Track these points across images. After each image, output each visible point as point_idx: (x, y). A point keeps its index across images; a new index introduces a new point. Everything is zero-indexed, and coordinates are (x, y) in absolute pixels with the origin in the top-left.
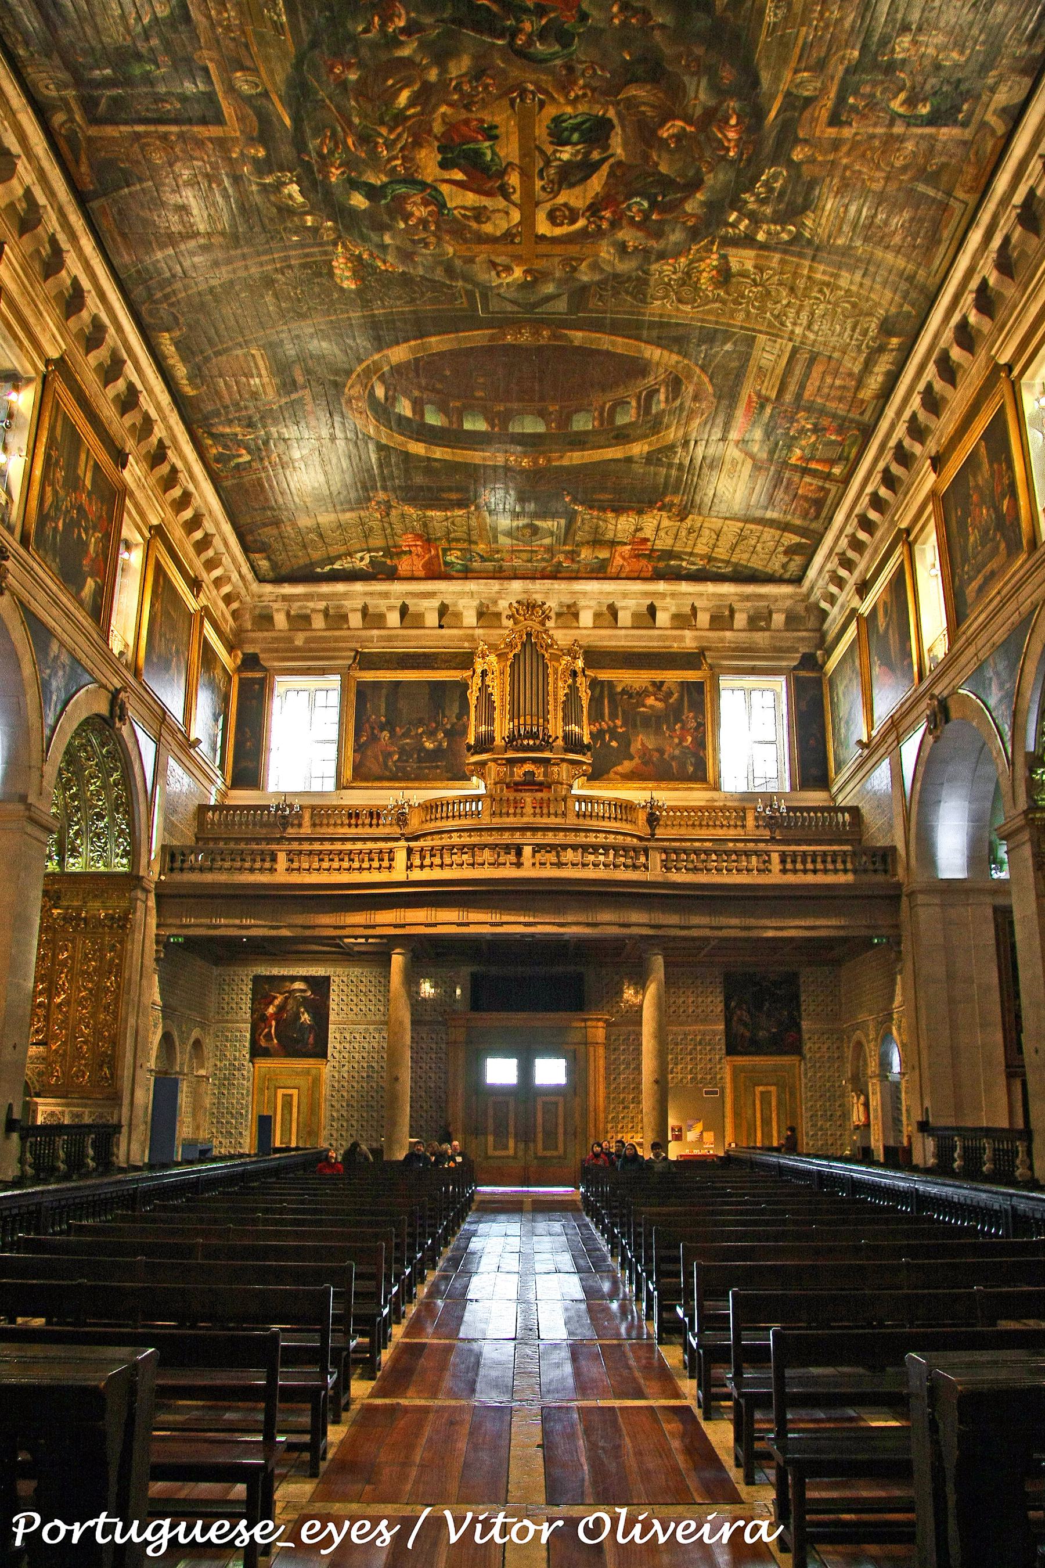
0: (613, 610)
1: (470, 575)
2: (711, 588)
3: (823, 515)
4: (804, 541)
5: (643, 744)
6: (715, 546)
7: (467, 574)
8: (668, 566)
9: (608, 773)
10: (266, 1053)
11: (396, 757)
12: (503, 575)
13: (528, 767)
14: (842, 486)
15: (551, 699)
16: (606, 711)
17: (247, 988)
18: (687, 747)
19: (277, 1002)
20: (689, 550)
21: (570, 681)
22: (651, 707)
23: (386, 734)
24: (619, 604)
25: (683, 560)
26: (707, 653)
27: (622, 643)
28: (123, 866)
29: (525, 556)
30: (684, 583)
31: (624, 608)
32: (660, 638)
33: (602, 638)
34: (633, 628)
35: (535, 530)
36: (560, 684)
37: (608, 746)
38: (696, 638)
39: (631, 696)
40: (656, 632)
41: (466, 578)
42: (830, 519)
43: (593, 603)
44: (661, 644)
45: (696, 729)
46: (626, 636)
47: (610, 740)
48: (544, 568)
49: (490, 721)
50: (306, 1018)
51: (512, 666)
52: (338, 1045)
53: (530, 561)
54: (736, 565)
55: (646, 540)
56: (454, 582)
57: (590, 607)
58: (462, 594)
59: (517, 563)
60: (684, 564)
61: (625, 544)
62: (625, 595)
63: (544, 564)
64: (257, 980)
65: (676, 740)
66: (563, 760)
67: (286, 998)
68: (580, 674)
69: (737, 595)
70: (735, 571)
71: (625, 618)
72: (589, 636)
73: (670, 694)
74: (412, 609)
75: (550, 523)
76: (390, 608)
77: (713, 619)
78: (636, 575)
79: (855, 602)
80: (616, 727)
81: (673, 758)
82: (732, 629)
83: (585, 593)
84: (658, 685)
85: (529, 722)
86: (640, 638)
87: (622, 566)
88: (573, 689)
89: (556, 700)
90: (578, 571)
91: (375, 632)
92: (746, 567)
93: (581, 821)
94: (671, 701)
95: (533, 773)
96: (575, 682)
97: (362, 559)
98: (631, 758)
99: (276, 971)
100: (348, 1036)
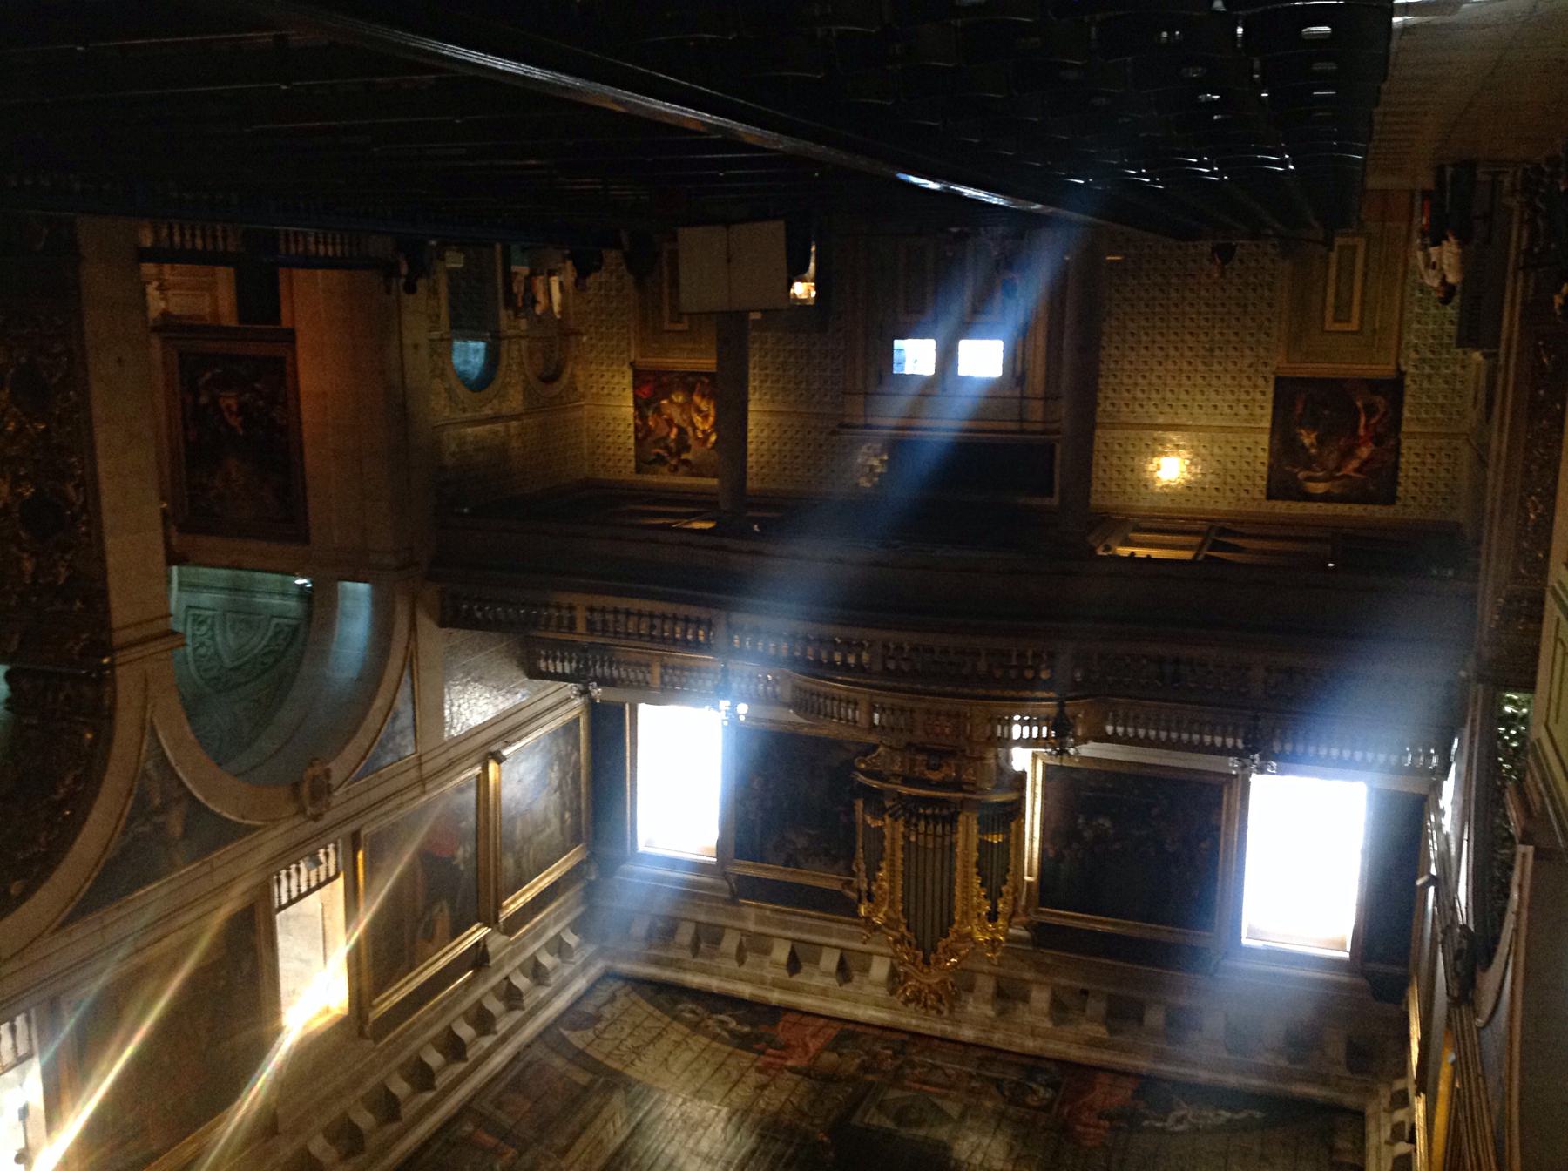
0: (844, 971)
2: (714, 984)
3: (520, 1065)
4: (566, 1033)
6: (678, 1044)
7: (1033, 1064)
8: (752, 1025)
10: (1374, 385)
11: (1155, 811)
12: (980, 1053)
13: (935, 776)
14: (475, 1105)
15: (899, 867)
17: (1405, 487)
19: (1355, 464)
20: (715, 1045)
21: (874, 888)
24: (832, 982)
25: (731, 1032)
26: (727, 896)
28: (1512, 702)
29: (937, 1077)
30: (747, 997)
31: (826, 974)
34: (821, 945)
35: (900, 1117)
38: (743, 918)
40: (790, 934)
42: (516, 1058)
43: (868, 989)
46: (830, 935)
48: (921, 1052)
49: (984, 846)
50: (1308, 439)
51: (951, 922)
52: (1259, 396)
53: (936, 1067)
54: (665, 1012)
55: (760, 1070)
56: (1056, 1055)
59: (952, 1068)
60: (733, 1024)
61: (792, 1070)
62: (824, 992)
63: (917, 1059)
64: (1391, 499)
67: (1338, 469)
68: (864, 895)
69: (685, 970)
70: (676, 1002)
71: (830, 961)
75: (875, 1122)
77: (716, 941)
78: (806, 1020)
79: (497, 942)
82: (698, 923)
83: (877, 1005)
84: (790, 861)
85: (930, 838)
87: (814, 1036)
88: (872, 878)
89: (892, 864)
90: (877, 1039)
92: (658, 1007)
93: (853, 695)
95: (929, 768)
96: (869, 885)
97: (1180, 1120)
99: (1357, 510)
100: (1243, 411)
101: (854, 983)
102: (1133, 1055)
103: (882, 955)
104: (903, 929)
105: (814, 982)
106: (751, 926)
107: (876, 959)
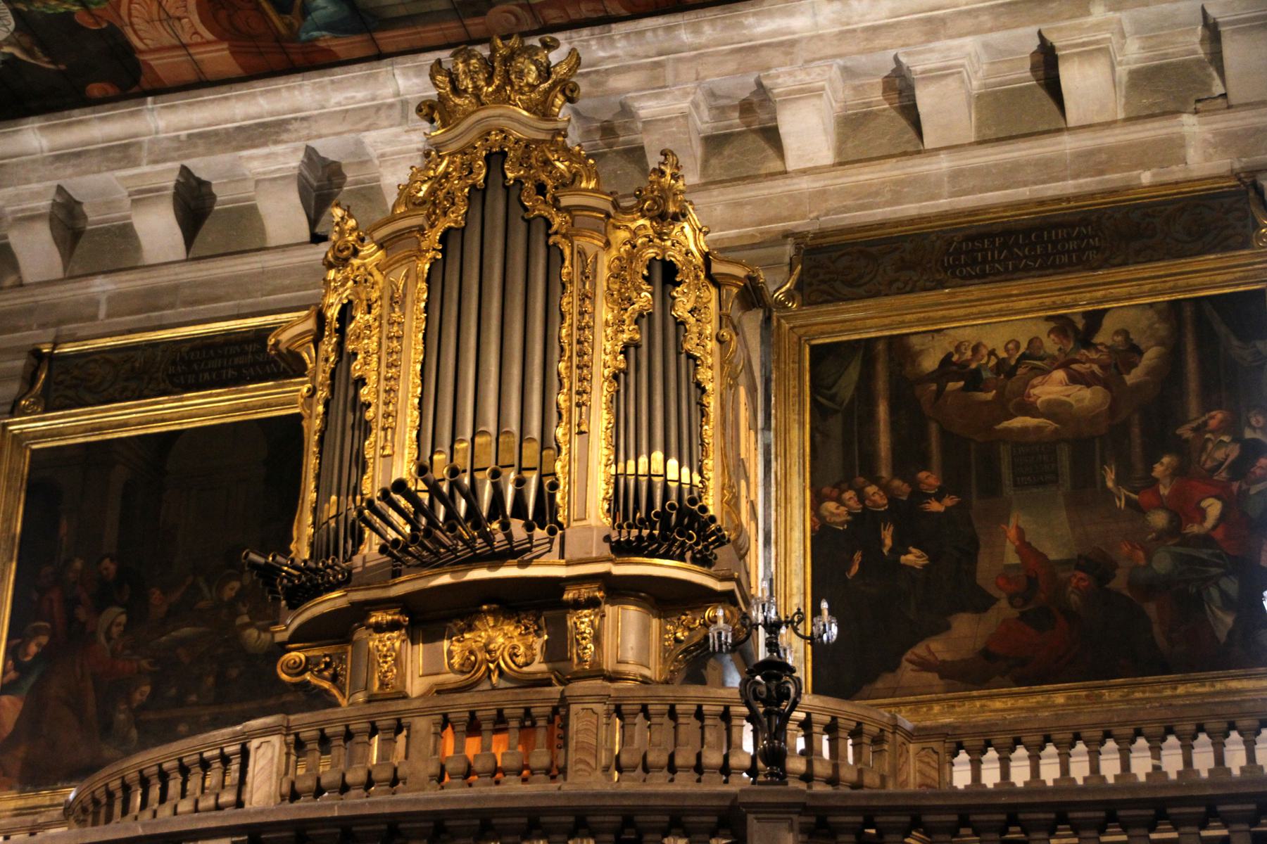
1: (387, 38)
5: (1025, 548)
9: (894, 667)
16: (884, 442)
18: (1206, 540)
21: (644, 298)
22: (1055, 410)
23: (116, 616)
24: (918, 64)
27: (944, 203)
32: (1090, 162)
33: (868, 195)
34: (981, 142)
36: (605, 312)
37: (893, 566)
38: (1227, 141)
39: (974, 380)
40: (1067, 144)
41: (379, 56)
43: (819, 75)
44: (1087, 183)
45: (1240, 468)
46: (956, 175)
47: (901, 546)
56: (340, 75)
57: (815, 92)
58: (370, 115)
65: (1159, 519)
66: (619, 590)
72: (822, 194)
73: (1133, 351)
74: (224, 195)
76: (142, 197)
80: (919, 495)
81: (1149, 588)
83: (788, 46)
86: (1009, 175)
91: (102, 286)
94: (1131, 378)
96: (667, 302)
98: (980, 602)
101: (879, 80)
102: (184, 133)
103: (804, 172)
104: (558, 221)
105: (970, 44)
106: (1189, 125)
107: (825, 154)
